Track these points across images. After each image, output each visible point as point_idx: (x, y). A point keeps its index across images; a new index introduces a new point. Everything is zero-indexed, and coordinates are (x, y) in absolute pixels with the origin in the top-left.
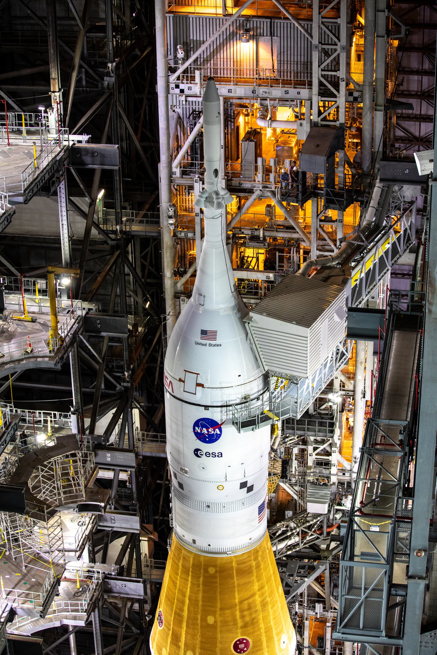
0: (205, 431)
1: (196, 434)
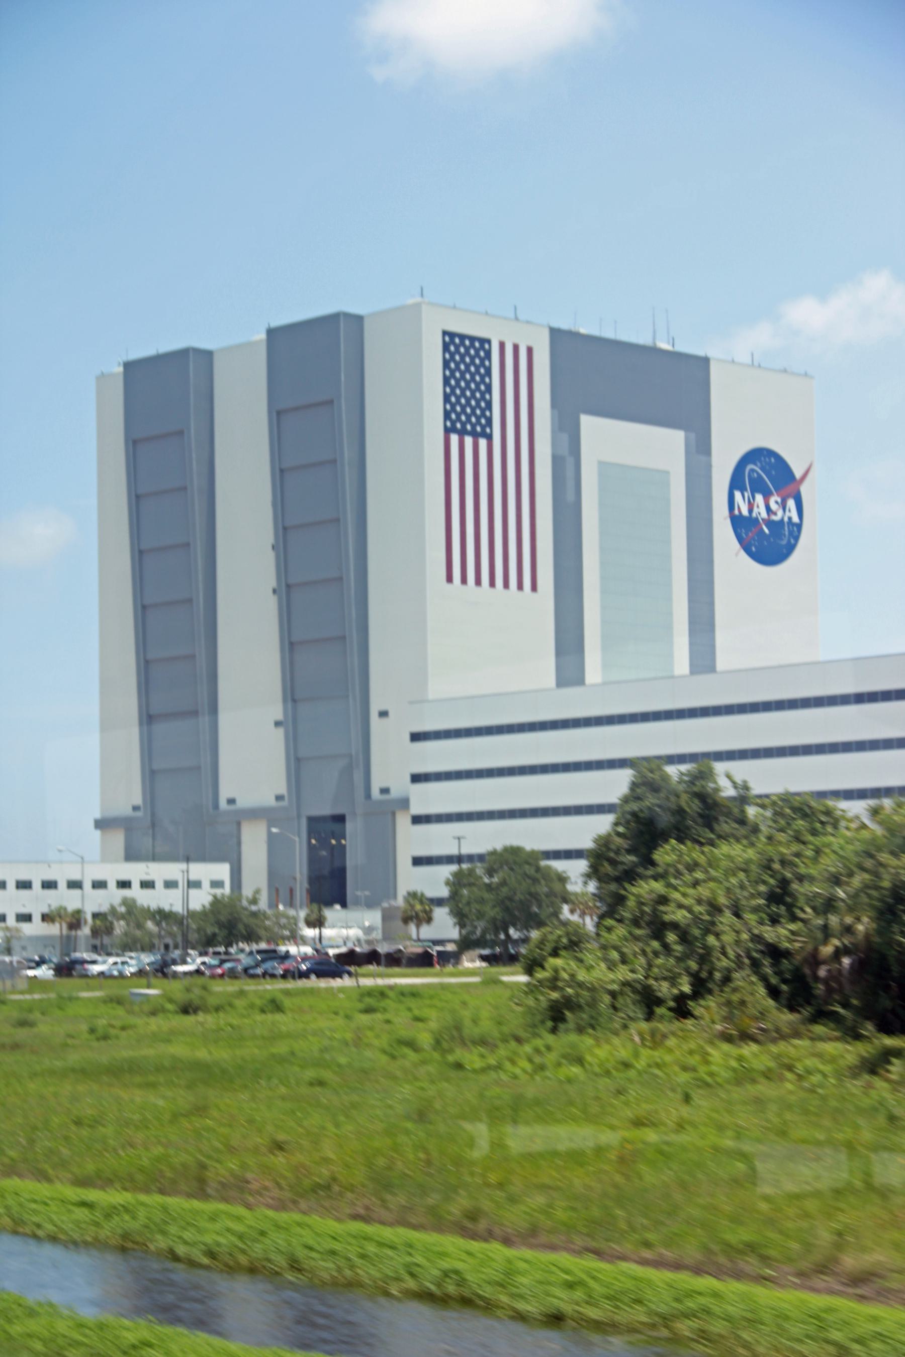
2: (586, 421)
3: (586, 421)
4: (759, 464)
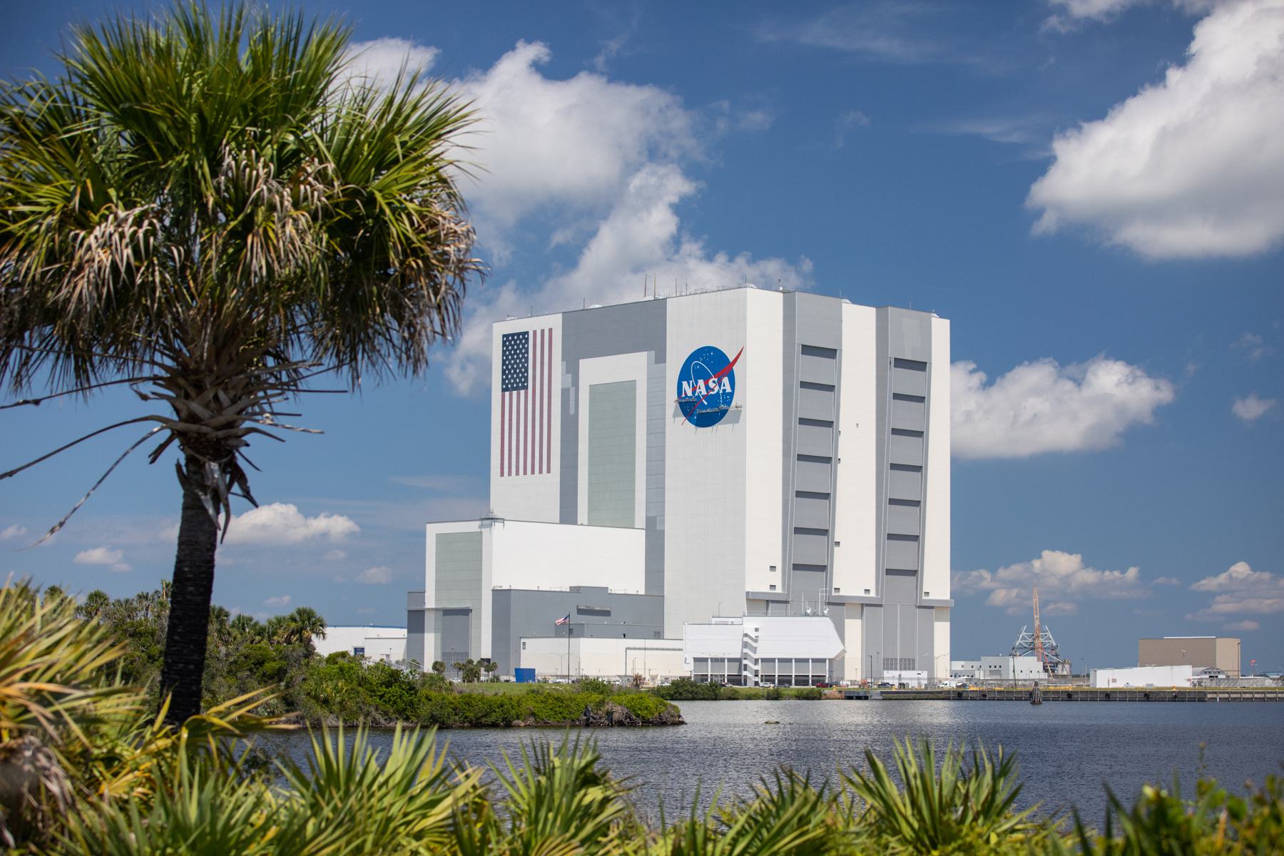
2: (585, 364)
3: (585, 364)
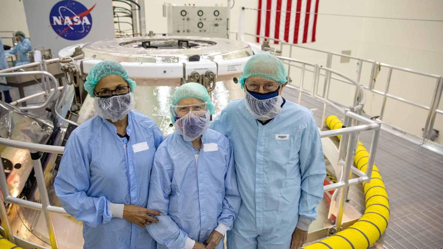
0: (68, 21)
1: (56, 28)
4: (66, 6)
